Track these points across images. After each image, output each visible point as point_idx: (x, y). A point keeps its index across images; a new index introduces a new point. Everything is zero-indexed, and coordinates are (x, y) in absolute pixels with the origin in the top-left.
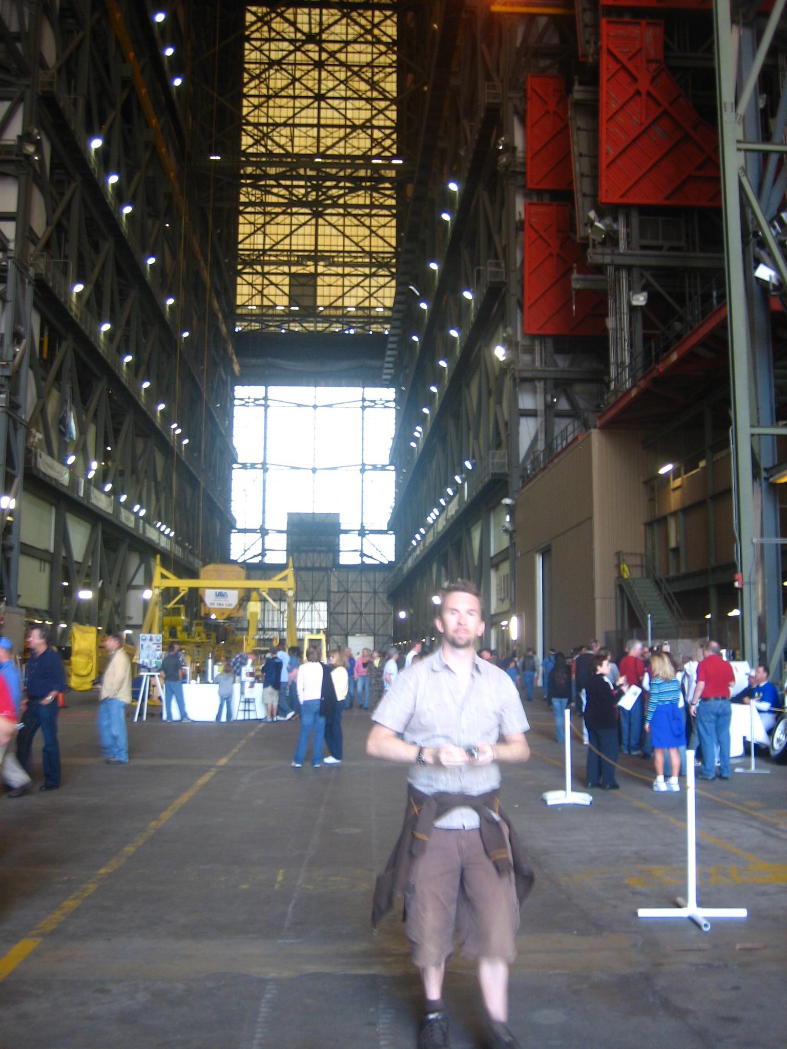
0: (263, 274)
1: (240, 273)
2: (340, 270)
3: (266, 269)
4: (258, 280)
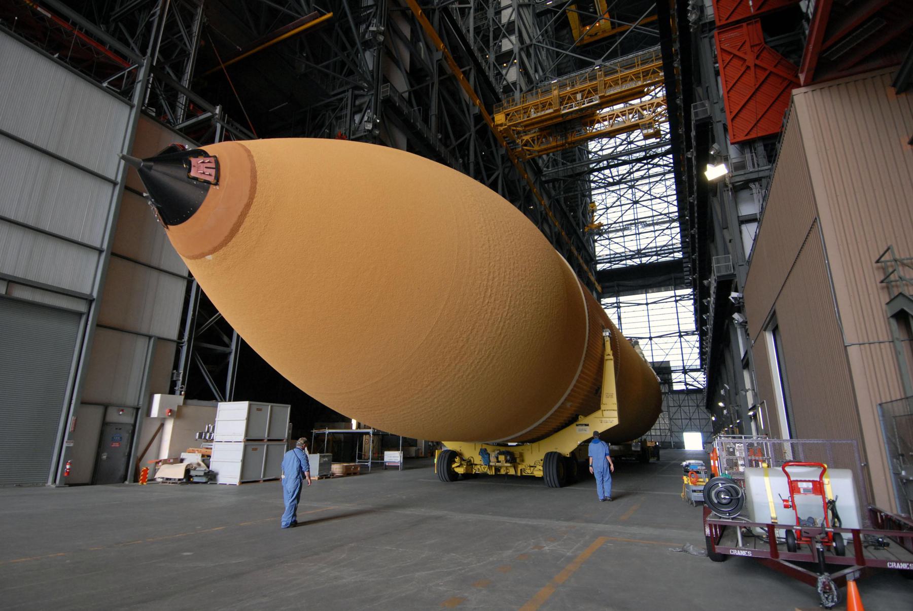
0: (609, 239)
1: (596, 241)
2: (651, 228)
3: (611, 235)
4: (606, 242)
